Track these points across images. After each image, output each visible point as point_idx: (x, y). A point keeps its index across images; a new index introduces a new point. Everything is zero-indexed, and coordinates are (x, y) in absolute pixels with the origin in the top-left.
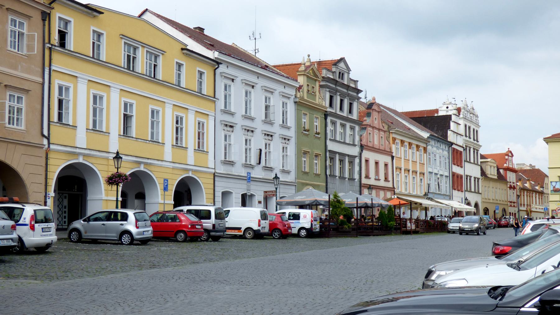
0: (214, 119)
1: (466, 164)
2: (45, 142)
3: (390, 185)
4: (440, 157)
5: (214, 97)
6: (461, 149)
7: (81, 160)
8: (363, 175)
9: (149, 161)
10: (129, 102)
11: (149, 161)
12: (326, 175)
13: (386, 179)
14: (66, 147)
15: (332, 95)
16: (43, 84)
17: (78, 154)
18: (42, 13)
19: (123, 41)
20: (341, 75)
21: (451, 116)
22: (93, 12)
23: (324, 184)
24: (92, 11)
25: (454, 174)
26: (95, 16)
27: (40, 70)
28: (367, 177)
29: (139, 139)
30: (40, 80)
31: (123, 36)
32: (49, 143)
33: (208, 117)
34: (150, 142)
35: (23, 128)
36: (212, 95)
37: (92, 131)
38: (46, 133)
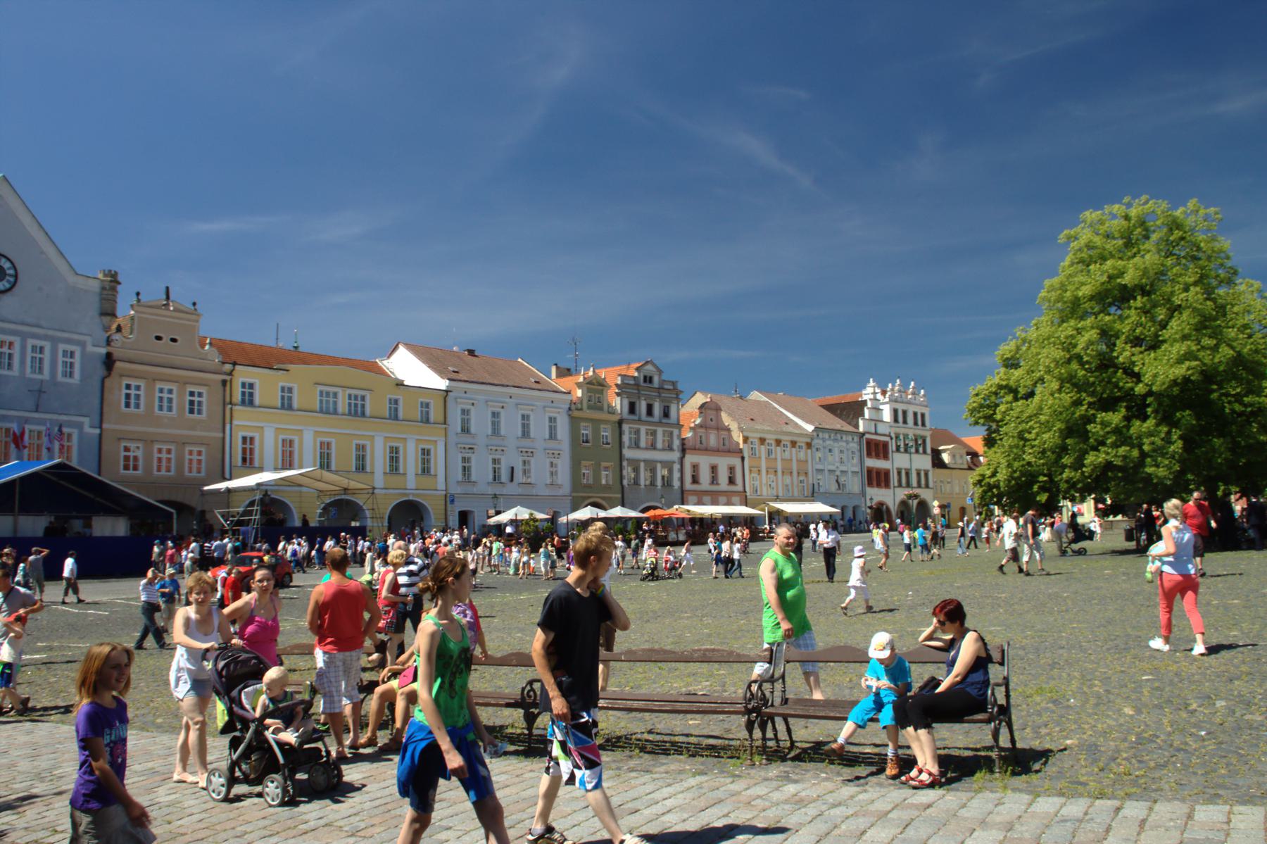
1: (896, 455)
3: (739, 488)
4: (841, 452)
6: (887, 439)
8: (688, 479)
12: (623, 487)
13: (731, 481)
15: (633, 400)
16: (224, 438)
20: (649, 379)
21: (866, 401)
23: (619, 496)
25: (870, 471)
27: (220, 426)
28: (695, 480)
30: (221, 435)
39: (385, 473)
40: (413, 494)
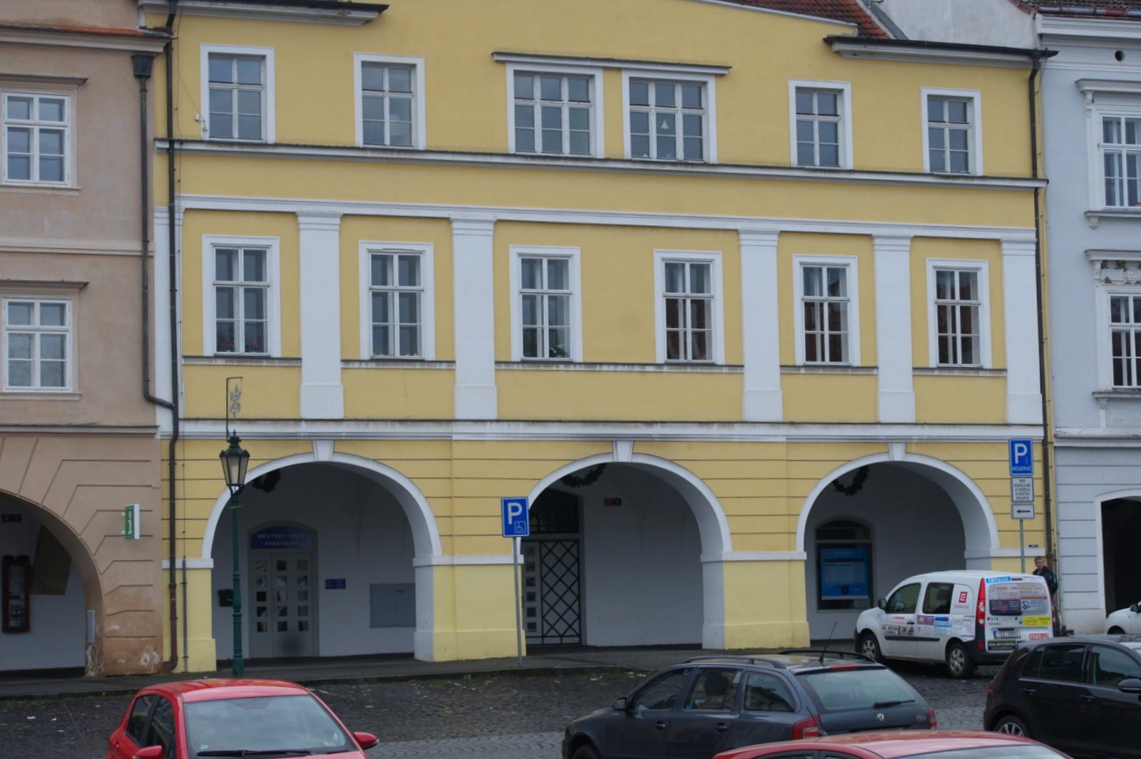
0: (1034, 253)
2: (163, 420)
5: (1034, 177)
7: (324, 454)
9: (656, 430)
10: (546, 256)
11: (656, 430)
14: (253, 422)
16: (145, 257)
17: (312, 439)
18: (133, 57)
19: (510, 70)
22: (347, 11)
24: (340, 11)
26: (368, 22)
27: (134, 220)
29: (601, 364)
30: (136, 246)
31: (502, 57)
32: (176, 420)
33: (1001, 250)
34: (665, 369)
35: (69, 388)
36: (1027, 172)
37: (372, 365)
38: (162, 390)
39: (787, 368)
40: (907, 441)
